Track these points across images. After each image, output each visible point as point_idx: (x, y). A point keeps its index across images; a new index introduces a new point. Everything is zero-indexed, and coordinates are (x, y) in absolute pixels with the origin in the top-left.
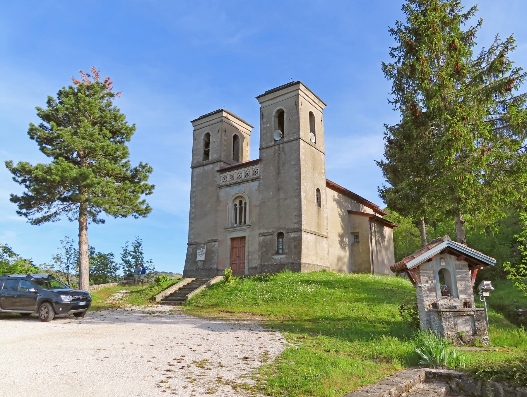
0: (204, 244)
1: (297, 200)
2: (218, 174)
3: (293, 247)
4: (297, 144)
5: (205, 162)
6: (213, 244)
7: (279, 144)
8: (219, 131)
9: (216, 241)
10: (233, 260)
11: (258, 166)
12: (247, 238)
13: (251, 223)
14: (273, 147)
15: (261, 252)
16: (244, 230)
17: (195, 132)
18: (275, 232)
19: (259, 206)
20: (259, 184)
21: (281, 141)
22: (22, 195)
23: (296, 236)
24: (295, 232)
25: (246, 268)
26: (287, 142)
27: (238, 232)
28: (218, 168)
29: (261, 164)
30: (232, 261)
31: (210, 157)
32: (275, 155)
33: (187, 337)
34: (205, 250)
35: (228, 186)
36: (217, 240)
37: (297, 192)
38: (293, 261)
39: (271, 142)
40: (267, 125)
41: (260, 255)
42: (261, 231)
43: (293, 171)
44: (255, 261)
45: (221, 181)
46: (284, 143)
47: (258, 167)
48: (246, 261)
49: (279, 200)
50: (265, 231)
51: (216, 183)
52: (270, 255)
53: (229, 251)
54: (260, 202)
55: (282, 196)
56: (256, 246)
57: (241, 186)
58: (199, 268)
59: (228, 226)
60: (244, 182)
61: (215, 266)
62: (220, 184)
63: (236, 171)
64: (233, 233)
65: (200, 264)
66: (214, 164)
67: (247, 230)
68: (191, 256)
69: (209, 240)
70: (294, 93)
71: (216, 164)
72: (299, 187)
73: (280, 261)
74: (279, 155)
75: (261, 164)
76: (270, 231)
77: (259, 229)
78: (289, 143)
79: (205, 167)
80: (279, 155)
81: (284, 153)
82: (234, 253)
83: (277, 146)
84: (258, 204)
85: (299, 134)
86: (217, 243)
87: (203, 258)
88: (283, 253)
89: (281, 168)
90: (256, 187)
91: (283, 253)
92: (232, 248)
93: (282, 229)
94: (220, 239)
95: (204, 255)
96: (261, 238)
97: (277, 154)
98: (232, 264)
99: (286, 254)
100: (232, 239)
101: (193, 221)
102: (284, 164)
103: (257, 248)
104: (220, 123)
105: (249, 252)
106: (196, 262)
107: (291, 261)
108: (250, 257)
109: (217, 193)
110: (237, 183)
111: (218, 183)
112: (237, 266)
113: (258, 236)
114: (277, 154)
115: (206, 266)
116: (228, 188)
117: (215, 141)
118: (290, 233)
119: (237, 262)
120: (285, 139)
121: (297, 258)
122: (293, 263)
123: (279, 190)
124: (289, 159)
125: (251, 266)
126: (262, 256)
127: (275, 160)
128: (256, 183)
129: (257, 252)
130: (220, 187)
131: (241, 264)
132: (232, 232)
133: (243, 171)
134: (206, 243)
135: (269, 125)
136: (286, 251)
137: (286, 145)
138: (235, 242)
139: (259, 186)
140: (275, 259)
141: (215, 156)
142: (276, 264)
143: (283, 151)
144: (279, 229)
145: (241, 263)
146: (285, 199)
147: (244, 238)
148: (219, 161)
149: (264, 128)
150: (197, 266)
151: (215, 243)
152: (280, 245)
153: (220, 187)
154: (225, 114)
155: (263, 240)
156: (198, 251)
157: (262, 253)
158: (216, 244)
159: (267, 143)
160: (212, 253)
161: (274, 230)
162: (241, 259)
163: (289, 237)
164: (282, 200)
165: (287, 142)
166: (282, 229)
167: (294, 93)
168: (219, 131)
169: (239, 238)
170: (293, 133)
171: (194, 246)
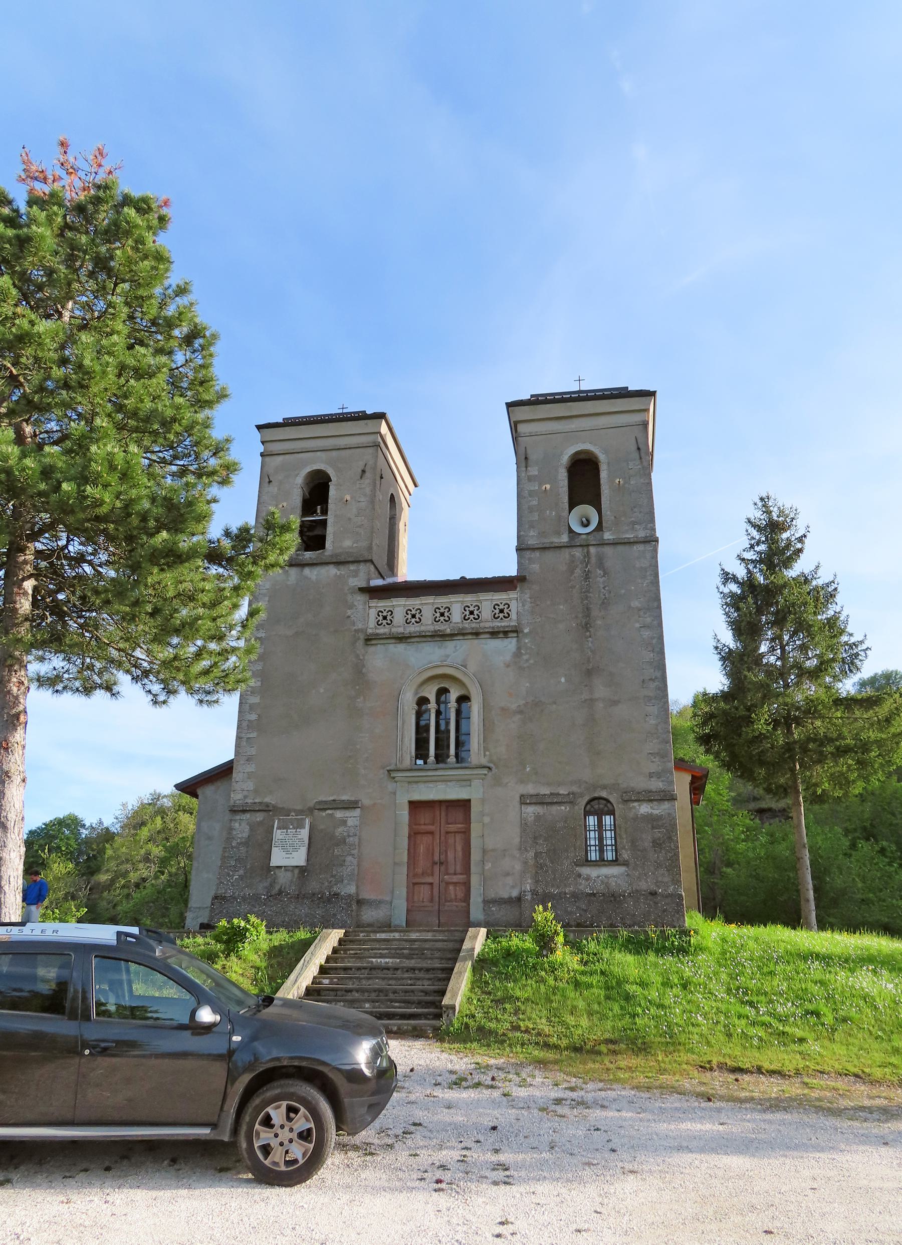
0: (300, 812)
1: (653, 710)
2: (360, 598)
3: (647, 844)
4: (648, 555)
5: (308, 555)
6: (339, 814)
7: (588, 545)
8: (364, 471)
9: (351, 805)
10: (419, 870)
11: (513, 595)
12: (475, 809)
13: (491, 761)
14: (567, 550)
15: (531, 854)
16: (466, 782)
17: (267, 459)
18: (582, 795)
19: (521, 712)
20: (519, 648)
21: (591, 537)
22: (217, 434)
23: (656, 812)
24: (651, 801)
25: (476, 899)
26: (614, 544)
27: (441, 786)
28: (359, 582)
29: (522, 592)
30: (415, 875)
31: (328, 544)
32: (572, 572)
33: (400, 1174)
34: (305, 833)
35: (402, 639)
36: (356, 802)
37: (653, 685)
38: (653, 888)
39: (558, 534)
40: (540, 485)
41: (531, 862)
42: (530, 789)
43: (637, 625)
44: (509, 880)
45: (372, 623)
46: (603, 544)
47: (510, 599)
48: (475, 880)
49: (590, 702)
50: (545, 791)
51: (354, 624)
52: (566, 863)
53: (404, 842)
54: (522, 702)
55: (601, 691)
56: (513, 835)
57: (450, 645)
58: (280, 892)
59: (401, 762)
60: (464, 634)
61: (352, 889)
62: (370, 631)
63: (430, 599)
64: (422, 786)
65: (283, 879)
66: (342, 567)
67: (476, 783)
68: (243, 849)
69: (325, 802)
70: (637, 418)
71: (352, 567)
72: (658, 674)
73: (607, 885)
74: (587, 576)
75: (522, 592)
76: (563, 791)
77: (522, 781)
78: (620, 548)
79: (307, 571)
80: (587, 576)
81: (605, 573)
82: (422, 849)
83: (580, 549)
84: (514, 707)
85: (654, 530)
86: (357, 812)
87: (299, 858)
88: (615, 862)
89: (595, 612)
90: (508, 657)
91: (602, 859)
92: (414, 835)
93: (604, 787)
94: (366, 802)
95: (303, 851)
96: (530, 809)
97: (578, 572)
98: (414, 884)
99: (626, 864)
100: (415, 806)
101: (254, 735)
102: (605, 604)
103: (517, 840)
104: (370, 450)
105: (484, 852)
106: (268, 869)
107: (644, 885)
108: (488, 866)
109: (357, 656)
110: (439, 636)
111: (360, 626)
112: (436, 890)
113: (517, 804)
114: (578, 572)
115: (313, 886)
116: (401, 647)
117: (348, 497)
118: (636, 804)
119: (435, 880)
120: (607, 536)
121: (666, 879)
122: (654, 894)
123: (589, 673)
124: (623, 591)
125: (492, 895)
126: (540, 867)
127: (573, 587)
128: (510, 644)
129: (517, 853)
130: (369, 640)
131: (451, 888)
132: (417, 782)
133: (399, 606)
134: (311, 811)
135: (548, 486)
136: (625, 855)
137: (608, 550)
138: (425, 817)
139: (518, 654)
140: (588, 878)
141: (347, 543)
142: (594, 895)
143: (601, 564)
144: (595, 787)
145: (448, 883)
146: (615, 703)
147: (465, 805)
148: (366, 561)
149: (532, 494)
150: (272, 885)
151: (348, 813)
152: (592, 833)
153: (369, 640)
154: (384, 429)
155: (538, 818)
156: (278, 834)
157: (537, 855)
158: (353, 817)
159: (542, 534)
160: (337, 845)
161: (575, 789)
162: (451, 871)
163: (631, 815)
164: (601, 705)
165: (614, 544)
166: (604, 787)
167: (637, 418)
168: (364, 471)
169: (440, 802)
170: (634, 523)
171: (259, 817)
